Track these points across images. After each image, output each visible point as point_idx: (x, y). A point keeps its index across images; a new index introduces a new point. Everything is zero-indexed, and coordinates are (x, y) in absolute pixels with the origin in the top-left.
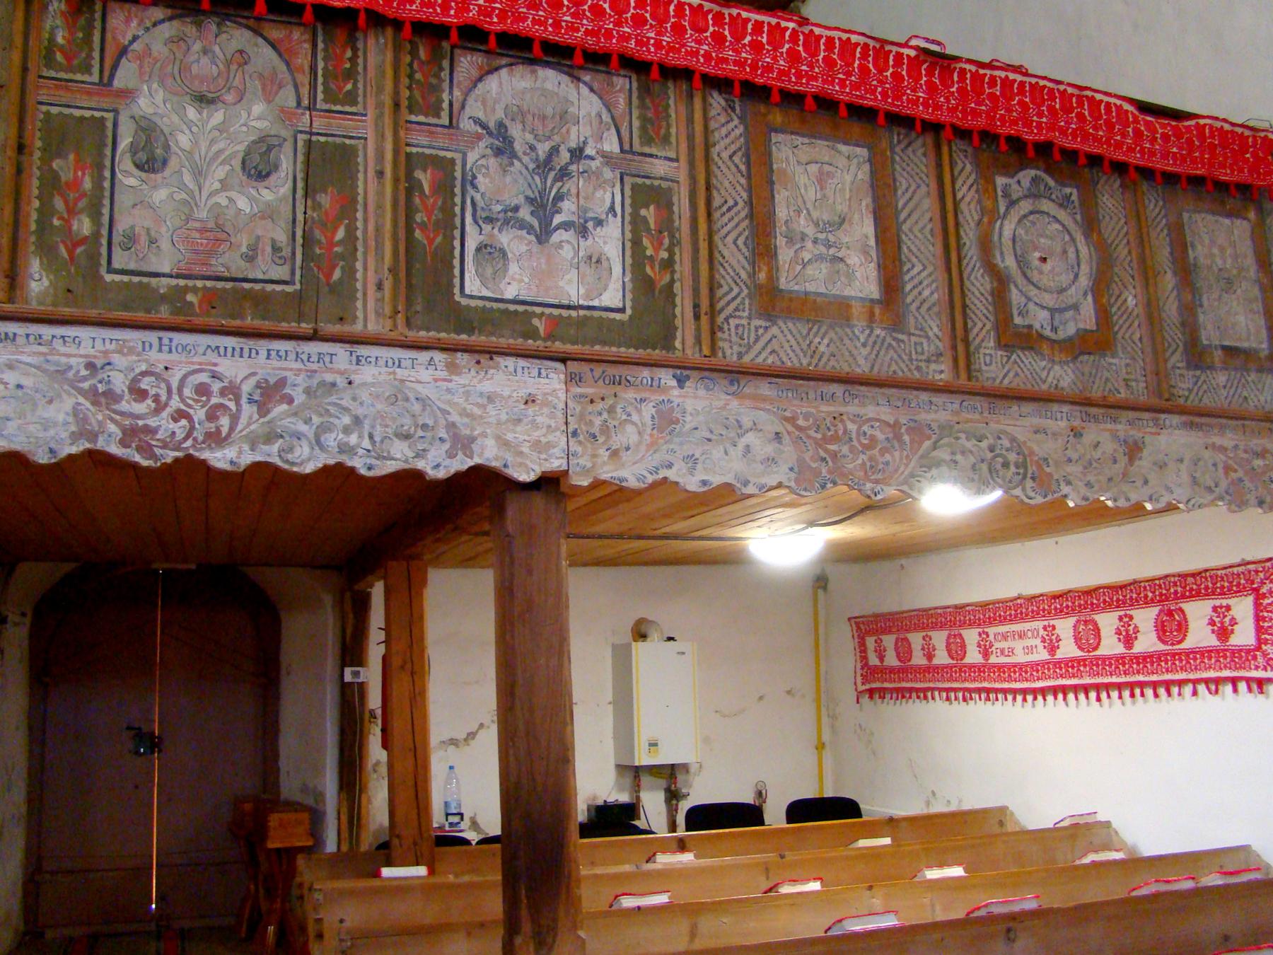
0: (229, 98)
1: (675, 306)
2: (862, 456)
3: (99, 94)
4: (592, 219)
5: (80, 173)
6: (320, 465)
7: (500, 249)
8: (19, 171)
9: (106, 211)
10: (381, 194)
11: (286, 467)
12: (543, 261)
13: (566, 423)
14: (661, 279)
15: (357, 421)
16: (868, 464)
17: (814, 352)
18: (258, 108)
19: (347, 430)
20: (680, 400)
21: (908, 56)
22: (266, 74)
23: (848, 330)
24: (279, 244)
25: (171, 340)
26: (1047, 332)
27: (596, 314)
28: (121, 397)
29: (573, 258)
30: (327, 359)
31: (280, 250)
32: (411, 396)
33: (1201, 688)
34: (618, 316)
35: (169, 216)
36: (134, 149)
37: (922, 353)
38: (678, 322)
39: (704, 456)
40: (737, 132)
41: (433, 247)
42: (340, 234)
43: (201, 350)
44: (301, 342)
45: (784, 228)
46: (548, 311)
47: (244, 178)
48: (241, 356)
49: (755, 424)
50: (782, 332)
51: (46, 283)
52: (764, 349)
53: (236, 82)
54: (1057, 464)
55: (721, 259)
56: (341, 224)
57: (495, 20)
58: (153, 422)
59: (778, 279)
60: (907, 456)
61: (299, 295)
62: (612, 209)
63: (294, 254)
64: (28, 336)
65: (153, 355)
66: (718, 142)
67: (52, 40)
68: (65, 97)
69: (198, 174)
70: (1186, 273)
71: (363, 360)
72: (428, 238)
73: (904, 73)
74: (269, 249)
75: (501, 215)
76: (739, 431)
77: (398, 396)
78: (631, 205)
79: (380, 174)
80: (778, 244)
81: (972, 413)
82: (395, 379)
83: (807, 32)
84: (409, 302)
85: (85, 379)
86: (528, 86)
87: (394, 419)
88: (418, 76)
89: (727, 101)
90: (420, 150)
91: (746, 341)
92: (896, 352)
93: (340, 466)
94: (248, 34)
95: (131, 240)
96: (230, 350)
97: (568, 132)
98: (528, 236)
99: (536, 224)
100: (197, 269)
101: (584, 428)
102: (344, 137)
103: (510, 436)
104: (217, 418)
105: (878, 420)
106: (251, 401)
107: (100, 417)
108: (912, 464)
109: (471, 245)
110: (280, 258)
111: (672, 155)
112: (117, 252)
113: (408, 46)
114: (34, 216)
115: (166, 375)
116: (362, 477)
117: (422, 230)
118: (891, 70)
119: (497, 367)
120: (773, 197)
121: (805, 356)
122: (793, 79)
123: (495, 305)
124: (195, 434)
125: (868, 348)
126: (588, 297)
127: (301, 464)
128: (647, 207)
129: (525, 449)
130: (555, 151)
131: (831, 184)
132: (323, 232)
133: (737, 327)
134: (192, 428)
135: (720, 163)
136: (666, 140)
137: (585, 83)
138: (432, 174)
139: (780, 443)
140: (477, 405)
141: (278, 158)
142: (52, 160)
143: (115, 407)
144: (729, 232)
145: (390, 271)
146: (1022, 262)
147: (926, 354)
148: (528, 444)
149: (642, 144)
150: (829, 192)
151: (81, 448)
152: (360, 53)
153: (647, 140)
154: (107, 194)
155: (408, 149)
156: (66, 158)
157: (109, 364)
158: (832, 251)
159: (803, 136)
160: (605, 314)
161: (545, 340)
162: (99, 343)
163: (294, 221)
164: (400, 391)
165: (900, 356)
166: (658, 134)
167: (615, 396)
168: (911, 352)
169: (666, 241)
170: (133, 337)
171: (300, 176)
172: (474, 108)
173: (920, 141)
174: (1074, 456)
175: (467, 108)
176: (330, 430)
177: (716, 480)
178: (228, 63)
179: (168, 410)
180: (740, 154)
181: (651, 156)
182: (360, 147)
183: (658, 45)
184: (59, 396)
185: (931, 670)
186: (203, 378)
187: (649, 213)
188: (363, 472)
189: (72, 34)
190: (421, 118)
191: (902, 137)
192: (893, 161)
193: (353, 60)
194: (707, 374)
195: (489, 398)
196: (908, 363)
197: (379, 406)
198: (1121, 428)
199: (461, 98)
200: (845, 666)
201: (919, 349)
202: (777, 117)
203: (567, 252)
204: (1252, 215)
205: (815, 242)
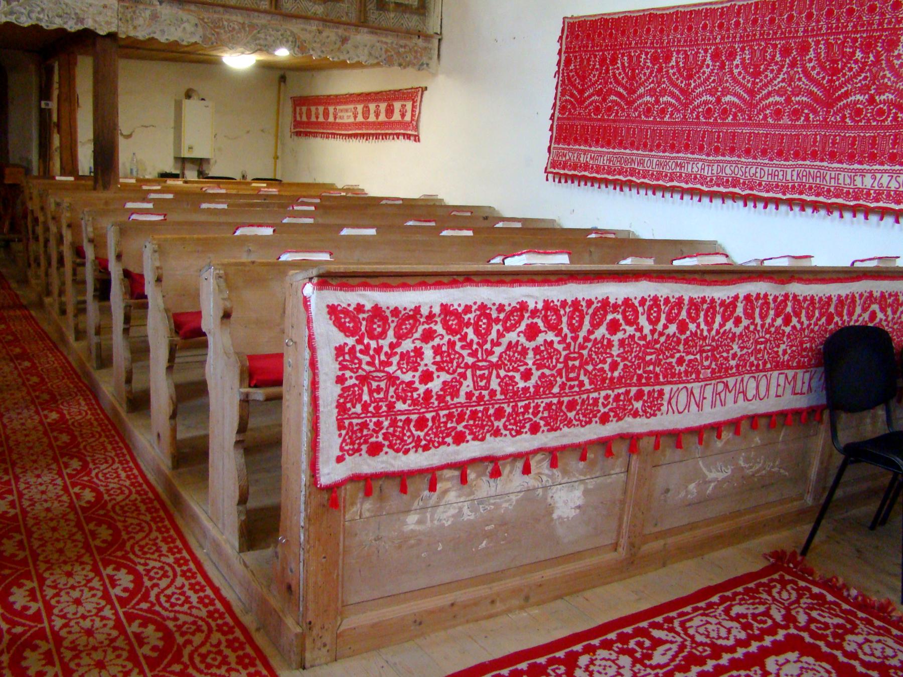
33: (401, 137)
103: (97, 19)
129: (103, 23)
174: (318, 40)
177: (172, 39)
185: (317, 124)
198: (340, 31)
200: (287, 120)
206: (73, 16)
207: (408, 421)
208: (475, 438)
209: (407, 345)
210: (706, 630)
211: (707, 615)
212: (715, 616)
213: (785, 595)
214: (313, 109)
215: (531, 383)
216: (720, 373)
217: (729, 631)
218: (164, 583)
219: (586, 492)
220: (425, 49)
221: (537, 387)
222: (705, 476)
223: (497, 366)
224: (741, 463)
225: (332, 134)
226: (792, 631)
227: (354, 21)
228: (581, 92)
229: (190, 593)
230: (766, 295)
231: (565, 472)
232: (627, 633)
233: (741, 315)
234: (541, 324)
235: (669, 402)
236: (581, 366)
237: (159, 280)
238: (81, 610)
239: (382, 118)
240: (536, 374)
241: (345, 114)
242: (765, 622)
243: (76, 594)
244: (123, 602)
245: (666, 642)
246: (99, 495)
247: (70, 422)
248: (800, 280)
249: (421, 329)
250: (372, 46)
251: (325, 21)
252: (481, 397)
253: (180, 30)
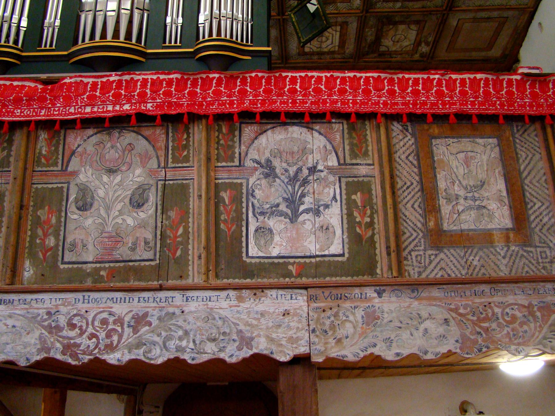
0: (124, 168)
1: (375, 248)
2: (506, 329)
3: (61, 176)
4: (322, 205)
5: (50, 216)
6: (166, 359)
7: (269, 229)
8: (20, 218)
9: (62, 233)
10: (200, 207)
11: (147, 361)
12: (294, 232)
13: (309, 325)
14: (366, 234)
15: (186, 333)
16: (511, 333)
17: (470, 266)
18: (138, 171)
19: (180, 339)
20: (380, 305)
21: (516, 79)
22: (142, 154)
23: (492, 249)
24: (148, 240)
25: (89, 296)
27: (327, 259)
28: (63, 328)
29: (312, 229)
30: (170, 300)
31: (149, 243)
32: (217, 317)
34: (340, 259)
35: (93, 232)
36: (76, 201)
37: (546, 258)
38: (378, 258)
39: (397, 338)
40: (410, 142)
41: (231, 232)
42: (181, 231)
43: (104, 300)
44: (156, 292)
45: (444, 193)
46: (297, 260)
47: (131, 208)
48: (125, 302)
49: (430, 315)
50: (447, 256)
51: (32, 272)
52: (435, 268)
53: (128, 160)
55: (404, 217)
56: (180, 227)
57: (259, 106)
58: (78, 341)
59: (442, 224)
60: (540, 326)
61: (159, 266)
62: (334, 198)
63: (156, 244)
64: (19, 300)
65: (80, 305)
66: (399, 150)
67: (40, 153)
68: (45, 179)
69: (108, 209)
71: (190, 299)
72: (228, 227)
73: (514, 90)
74: (143, 244)
75: (269, 210)
76: (420, 320)
77: (209, 317)
78: (346, 194)
79: (200, 196)
80: (441, 203)
82: (208, 308)
83: (447, 78)
84: (217, 264)
85: (46, 320)
86: (283, 137)
87: (207, 331)
88: (222, 142)
89: (402, 126)
90: (223, 181)
91: (423, 264)
92: (527, 259)
93: (177, 359)
94: (134, 135)
95: (74, 245)
96: (119, 299)
97: (307, 159)
98: (285, 220)
99: (289, 212)
100: (106, 258)
101: (319, 326)
102: (183, 180)
103: (274, 336)
104: (111, 336)
105: (515, 304)
106: (129, 326)
107: (52, 340)
108: (545, 330)
109: (252, 229)
110: (149, 247)
111: (370, 162)
112: (67, 252)
113: (217, 127)
114: (28, 239)
115: (86, 315)
116: (189, 364)
117: (224, 223)
118: (505, 90)
119: (266, 296)
120: (436, 176)
121: (464, 269)
122: (441, 107)
123: (266, 261)
124: (100, 346)
125: (507, 259)
126: (321, 250)
127: (156, 359)
128: (356, 194)
129: (284, 343)
130: (300, 170)
131: (473, 163)
132: (171, 231)
133: (416, 257)
134: (98, 343)
135: (401, 162)
136: (366, 154)
137: (316, 130)
138: (230, 193)
139: (448, 325)
140: (255, 319)
141: (148, 196)
142: (37, 210)
143: (60, 334)
144: (408, 201)
145: (204, 248)
147: (549, 257)
148: (286, 339)
149: (351, 159)
150: (472, 168)
151: (42, 357)
152: (191, 135)
153: (354, 155)
154: (63, 224)
155: (217, 181)
156: (44, 208)
157: (58, 311)
158: (477, 203)
159: (453, 138)
160: (331, 259)
161: (296, 277)
162: (53, 300)
163: (156, 227)
164: (210, 314)
165: (530, 262)
166: (360, 152)
167: (339, 306)
168: (538, 258)
169: (369, 212)
170: (70, 296)
171: (159, 203)
172: (253, 154)
173: (532, 128)
175: (249, 155)
176: (172, 339)
177: (405, 352)
178: (124, 151)
179: (87, 334)
180: (413, 154)
181: (357, 164)
182: (191, 184)
183: (355, 102)
184: (34, 330)
186: (105, 315)
187: (358, 197)
188: (190, 361)
189: (49, 148)
190: (224, 164)
191: (519, 128)
192: (514, 142)
193: (188, 139)
194: (396, 287)
195: (261, 314)
196: (537, 265)
197: (199, 324)
199: (245, 150)
201: (544, 255)
202: (435, 130)
203: (308, 226)
205: (466, 198)
206: (235, 337)
253: (418, 334)
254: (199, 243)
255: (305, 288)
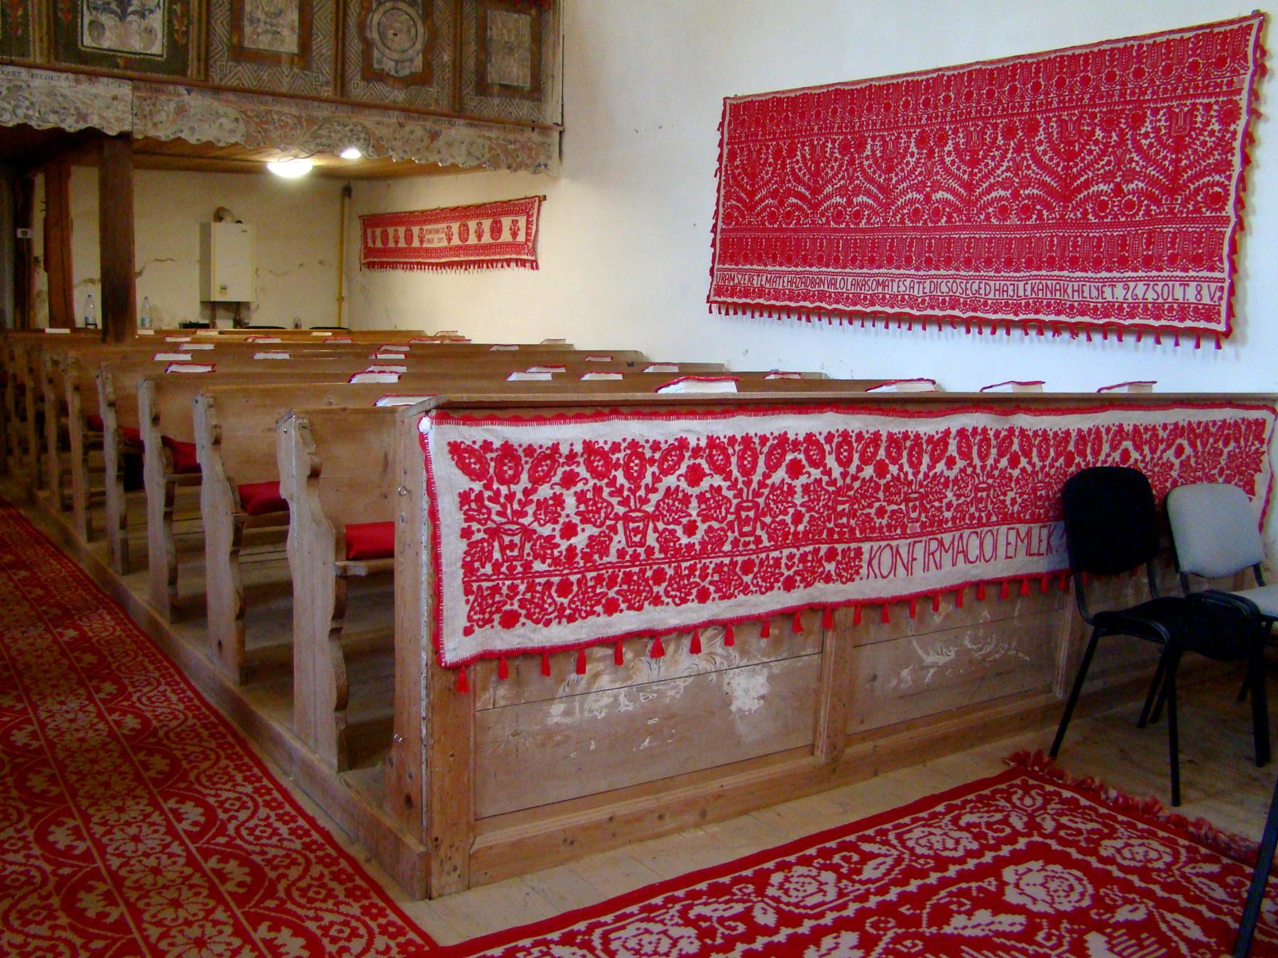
15: (32, 104)
19: (28, 108)
26: (393, 73)
33: (513, 264)
54: (388, 140)
62: (158, 5)
70: (483, 43)
81: (342, 113)
93: (25, 125)
109: (86, 21)
146: (382, 36)
177: (204, 139)
185: (397, 251)
198: (429, 125)
200: (355, 247)
203: (135, 26)
204: (534, 12)
206: (73, 111)
207: (548, 585)
208: (630, 608)
209: (544, 491)
210: (929, 841)
211: (930, 826)
212: (940, 827)
213: (1028, 801)
214: (391, 231)
215: (696, 539)
216: (933, 526)
217: (957, 842)
218: (243, 815)
219: (771, 679)
220: (542, 144)
221: (703, 543)
222: (921, 660)
223: (654, 517)
224: (967, 643)
225: (418, 263)
226: (1036, 838)
227: (445, 110)
228: (751, 195)
229: (278, 824)
230: (985, 430)
231: (744, 653)
232: (831, 848)
233: (955, 454)
234: (705, 466)
235: (870, 564)
236: (757, 518)
237: (217, 442)
238: (142, 848)
239: (487, 239)
240: (702, 527)
241: (436, 237)
242: (1002, 831)
243: (133, 830)
244: (194, 837)
245: (878, 855)
246: (146, 722)
247: (94, 640)
248: (1028, 411)
249: (560, 471)
250: (472, 144)
251: (408, 111)
252: (635, 556)
253: (215, 127)
254: (41, 27)
255: (131, 79)
